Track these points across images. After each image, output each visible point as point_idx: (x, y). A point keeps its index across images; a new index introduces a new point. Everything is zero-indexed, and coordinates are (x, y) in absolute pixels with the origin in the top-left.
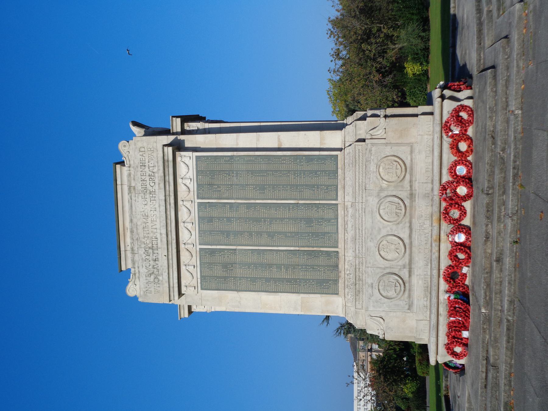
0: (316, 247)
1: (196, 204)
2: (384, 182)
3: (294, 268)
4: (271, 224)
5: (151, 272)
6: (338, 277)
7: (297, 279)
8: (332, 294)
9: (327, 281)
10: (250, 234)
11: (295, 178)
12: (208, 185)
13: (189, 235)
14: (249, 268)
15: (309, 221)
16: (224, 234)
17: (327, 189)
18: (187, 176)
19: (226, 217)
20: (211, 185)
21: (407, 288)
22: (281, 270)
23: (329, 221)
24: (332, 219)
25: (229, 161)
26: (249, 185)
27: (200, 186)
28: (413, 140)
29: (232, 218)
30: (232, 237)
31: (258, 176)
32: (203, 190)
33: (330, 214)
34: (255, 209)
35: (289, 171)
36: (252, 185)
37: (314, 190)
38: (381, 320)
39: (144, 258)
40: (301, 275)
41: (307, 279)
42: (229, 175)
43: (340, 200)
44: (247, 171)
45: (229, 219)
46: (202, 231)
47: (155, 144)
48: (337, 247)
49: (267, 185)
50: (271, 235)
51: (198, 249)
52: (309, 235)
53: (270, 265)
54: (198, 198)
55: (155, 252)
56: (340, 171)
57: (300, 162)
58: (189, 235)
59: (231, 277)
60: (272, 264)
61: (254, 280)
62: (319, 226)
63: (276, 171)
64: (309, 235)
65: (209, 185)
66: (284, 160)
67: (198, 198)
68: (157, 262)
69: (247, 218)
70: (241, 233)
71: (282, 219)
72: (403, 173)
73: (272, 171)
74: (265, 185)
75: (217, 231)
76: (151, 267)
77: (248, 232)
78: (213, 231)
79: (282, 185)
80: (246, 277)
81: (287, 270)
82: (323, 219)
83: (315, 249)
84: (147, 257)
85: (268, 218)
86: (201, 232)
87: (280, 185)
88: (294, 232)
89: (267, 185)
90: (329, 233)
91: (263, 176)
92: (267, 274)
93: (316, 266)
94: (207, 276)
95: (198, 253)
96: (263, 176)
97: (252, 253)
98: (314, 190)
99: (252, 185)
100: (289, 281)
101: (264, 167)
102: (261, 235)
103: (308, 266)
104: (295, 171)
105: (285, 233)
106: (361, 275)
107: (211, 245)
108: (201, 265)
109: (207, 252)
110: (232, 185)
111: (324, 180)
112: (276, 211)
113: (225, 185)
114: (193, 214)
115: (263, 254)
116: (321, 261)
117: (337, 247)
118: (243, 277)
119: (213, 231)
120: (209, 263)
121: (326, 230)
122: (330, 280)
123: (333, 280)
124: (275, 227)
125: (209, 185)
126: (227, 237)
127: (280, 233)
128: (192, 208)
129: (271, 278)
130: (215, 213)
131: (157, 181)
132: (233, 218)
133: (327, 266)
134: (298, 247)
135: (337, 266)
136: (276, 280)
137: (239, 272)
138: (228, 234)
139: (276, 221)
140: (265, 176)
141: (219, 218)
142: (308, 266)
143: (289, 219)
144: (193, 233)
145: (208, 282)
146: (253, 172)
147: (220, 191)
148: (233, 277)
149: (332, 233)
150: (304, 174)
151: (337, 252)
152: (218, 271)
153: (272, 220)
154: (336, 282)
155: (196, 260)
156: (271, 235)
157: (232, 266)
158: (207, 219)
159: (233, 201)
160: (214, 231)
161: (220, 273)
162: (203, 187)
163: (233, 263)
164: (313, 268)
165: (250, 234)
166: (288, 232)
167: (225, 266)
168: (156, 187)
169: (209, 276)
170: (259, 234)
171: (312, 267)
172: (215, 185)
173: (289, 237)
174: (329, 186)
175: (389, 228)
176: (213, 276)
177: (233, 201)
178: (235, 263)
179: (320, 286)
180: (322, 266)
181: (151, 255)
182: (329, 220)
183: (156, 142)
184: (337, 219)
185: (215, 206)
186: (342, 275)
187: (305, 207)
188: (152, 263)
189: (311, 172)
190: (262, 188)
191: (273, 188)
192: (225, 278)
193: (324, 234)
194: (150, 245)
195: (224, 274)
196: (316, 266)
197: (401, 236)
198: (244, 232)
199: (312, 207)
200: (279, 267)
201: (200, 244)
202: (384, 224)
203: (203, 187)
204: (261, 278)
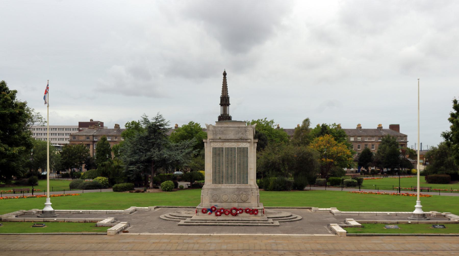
10: (228, 161)
15: (231, 176)
27: (240, 148)
33: (233, 182)
40: (217, 174)
45: (231, 156)
50: (228, 167)
53: (219, 166)
61: (216, 162)
62: (230, 179)
70: (228, 159)
86: (228, 148)
92: (217, 165)
101: (245, 165)
111: (242, 181)
116: (221, 180)
130: (233, 152)
135: (220, 183)
136: (216, 168)
137: (218, 158)
138: (228, 155)
145: (214, 149)
152: (218, 152)
153: (231, 167)
154: (216, 183)
155: (220, 146)
156: (228, 167)
158: (232, 149)
161: (217, 152)
165: (228, 161)
167: (219, 154)
170: (228, 164)
190: (240, 164)
200: (219, 168)
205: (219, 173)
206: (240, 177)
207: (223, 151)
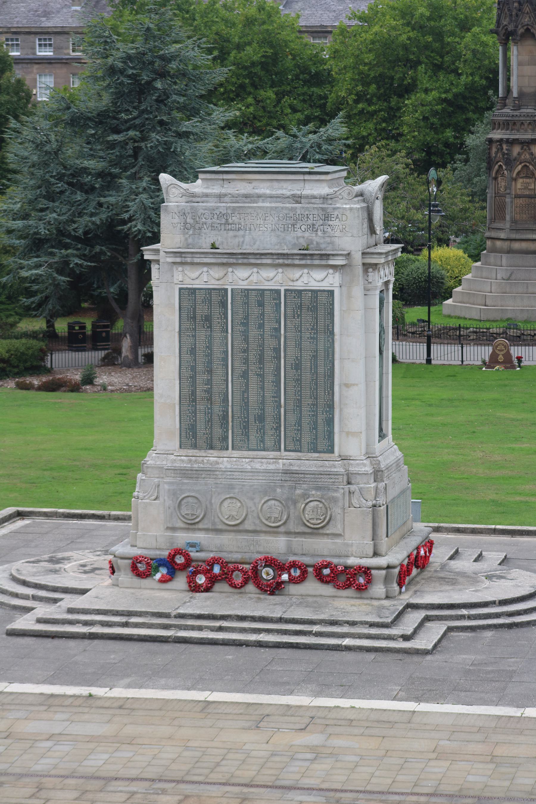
0: (232, 426)
1: (279, 288)
2: (303, 505)
3: (208, 400)
4: (258, 375)
5: (198, 219)
6: (200, 449)
7: (196, 403)
8: (180, 441)
9: (195, 436)
10: (246, 351)
11: (308, 404)
12: (301, 303)
13: (242, 278)
14: (207, 347)
15: (261, 418)
16: (245, 319)
17: (297, 440)
18: (311, 279)
19: (264, 323)
20: (300, 307)
21: (191, 527)
22: (206, 385)
23: (262, 441)
24: (264, 445)
25: (328, 329)
26: (301, 352)
27: (300, 292)
28: (347, 535)
29: (264, 330)
30: (242, 328)
31: (311, 363)
32: (295, 297)
33: (269, 442)
34: (274, 357)
35: (317, 399)
36: (301, 355)
37: (295, 426)
38: (153, 497)
39: (214, 212)
40: (201, 407)
41: (196, 414)
42: (312, 329)
43: (284, 453)
44: (317, 351)
45: (261, 326)
46: (248, 293)
47: (350, 235)
48: (233, 449)
49: (301, 372)
50: (245, 375)
51: (226, 287)
52: (245, 418)
53: (210, 372)
54: (286, 290)
55: (223, 227)
56: (317, 455)
57: (326, 412)
58: (242, 278)
59: (195, 326)
60: (211, 375)
61: (193, 351)
63: (316, 384)
64: (245, 418)
65: (301, 305)
66: (329, 393)
67: (286, 290)
68: (210, 228)
69: (263, 348)
70: (246, 340)
71: (263, 388)
72: (312, 526)
73: (316, 379)
74: (301, 370)
75: (248, 311)
76: (204, 220)
77: (248, 347)
78: (248, 307)
79: (301, 390)
80: (195, 343)
81: (205, 391)
82: (264, 434)
83: (230, 424)
84: (216, 216)
85: (263, 372)
87: (301, 388)
88: (248, 402)
89: (301, 372)
90: (248, 440)
91: (311, 369)
92: (200, 367)
93: (211, 425)
94: (195, 297)
95: (223, 287)
96: (311, 369)
97: (224, 352)
98: (295, 426)
99: (301, 355)
100: (194, 393)
102: (244, 363)
103: (211, 416)
104: (317, 406)
105: (247, 390)
106: (203, 476)
107: (232, 303)
108: (209, 289)
109: (223, 298)
110: (300, 331)
111: (306, 438)
112: (273, 382)
113: (301, 323)
114: (267, 283)
115: (223, 365)
116: (217, 431)
117: (233, 449)
118: (195, 340)
119: (248, 307)
120: (211, 299)
121: (252, 438)
122: (196, 440)
123: (196, 443)
124: (253, 380)
125: (301, 305)
126: (241, 323)
127: (247, 385)
128: (275, 283)
129: (196, 372)
130: (268, 309)
131: (307, 234)
132: (263, 331)
133: (212, 437)
134: (232, 405)
135: (212, 448)
136: (193, 378)
138: (245, 324)
139: (261, 381)
140: (311, 370)
141: (263, 314)
142: (211, 416)
143: (263, 396)
144: (245, 283)
145: (188, 294)
146: (315, 357)
147: (294, 318)
148: (195, 328)
149: (248, 444)
150: (313, 415)
151: (227, 449)
152: (202, 310)
154: (195, 446)
157: (208, 327)
159: (282, 332)
160: (248, 309)
162: (298, 297)
163: (211, 328)
164: (208, 422)
166: (248, 395)
167: (208, 319)
168: (300, 234)
169: (195, 299)
170: (246, 361)
171: (210, 420)
172: (301, 312)
173: (243, 395)
174: (300, 442)
175: (254, 508)
176: (195, 304)
177: (282, 332)
178: (211, 331)
179: (189, 429)
180: (212, 431)
181: (218, 221)
182: (262, 441)
183: (352, 236)
184: (264, 450)
185: (276, 310)
186: (202, 453)
187: (276, 415)
188: (209, 221)
189: (316, 423)
191: (298, 380)
192: (194, 318)
193: (247, 435)
194: (230, 221)
195: (198, 317)
196: (211, 425)
197: (246, 522)
198: (248, 344)
199: (277, 423)
200: (209, 382)
201: (232, 289)
202: (259, 503)
203: (298, 297)
204: (196, 361)
205: (210, 399)
206: (299, 423)
207: (224, 304)
